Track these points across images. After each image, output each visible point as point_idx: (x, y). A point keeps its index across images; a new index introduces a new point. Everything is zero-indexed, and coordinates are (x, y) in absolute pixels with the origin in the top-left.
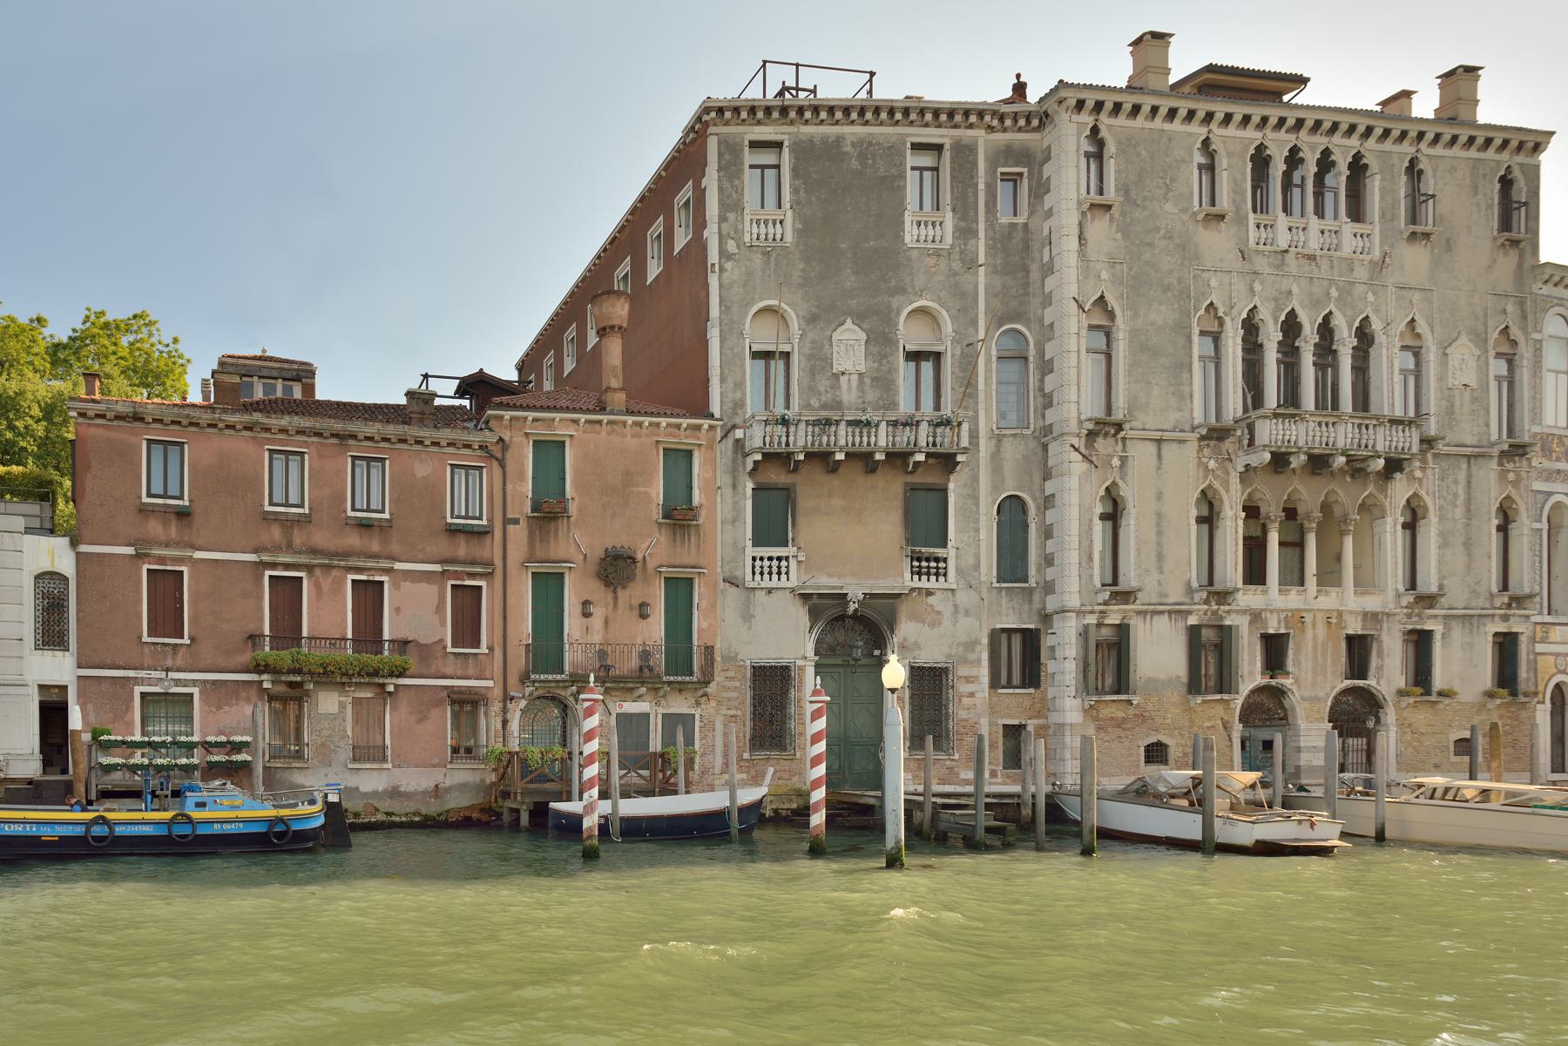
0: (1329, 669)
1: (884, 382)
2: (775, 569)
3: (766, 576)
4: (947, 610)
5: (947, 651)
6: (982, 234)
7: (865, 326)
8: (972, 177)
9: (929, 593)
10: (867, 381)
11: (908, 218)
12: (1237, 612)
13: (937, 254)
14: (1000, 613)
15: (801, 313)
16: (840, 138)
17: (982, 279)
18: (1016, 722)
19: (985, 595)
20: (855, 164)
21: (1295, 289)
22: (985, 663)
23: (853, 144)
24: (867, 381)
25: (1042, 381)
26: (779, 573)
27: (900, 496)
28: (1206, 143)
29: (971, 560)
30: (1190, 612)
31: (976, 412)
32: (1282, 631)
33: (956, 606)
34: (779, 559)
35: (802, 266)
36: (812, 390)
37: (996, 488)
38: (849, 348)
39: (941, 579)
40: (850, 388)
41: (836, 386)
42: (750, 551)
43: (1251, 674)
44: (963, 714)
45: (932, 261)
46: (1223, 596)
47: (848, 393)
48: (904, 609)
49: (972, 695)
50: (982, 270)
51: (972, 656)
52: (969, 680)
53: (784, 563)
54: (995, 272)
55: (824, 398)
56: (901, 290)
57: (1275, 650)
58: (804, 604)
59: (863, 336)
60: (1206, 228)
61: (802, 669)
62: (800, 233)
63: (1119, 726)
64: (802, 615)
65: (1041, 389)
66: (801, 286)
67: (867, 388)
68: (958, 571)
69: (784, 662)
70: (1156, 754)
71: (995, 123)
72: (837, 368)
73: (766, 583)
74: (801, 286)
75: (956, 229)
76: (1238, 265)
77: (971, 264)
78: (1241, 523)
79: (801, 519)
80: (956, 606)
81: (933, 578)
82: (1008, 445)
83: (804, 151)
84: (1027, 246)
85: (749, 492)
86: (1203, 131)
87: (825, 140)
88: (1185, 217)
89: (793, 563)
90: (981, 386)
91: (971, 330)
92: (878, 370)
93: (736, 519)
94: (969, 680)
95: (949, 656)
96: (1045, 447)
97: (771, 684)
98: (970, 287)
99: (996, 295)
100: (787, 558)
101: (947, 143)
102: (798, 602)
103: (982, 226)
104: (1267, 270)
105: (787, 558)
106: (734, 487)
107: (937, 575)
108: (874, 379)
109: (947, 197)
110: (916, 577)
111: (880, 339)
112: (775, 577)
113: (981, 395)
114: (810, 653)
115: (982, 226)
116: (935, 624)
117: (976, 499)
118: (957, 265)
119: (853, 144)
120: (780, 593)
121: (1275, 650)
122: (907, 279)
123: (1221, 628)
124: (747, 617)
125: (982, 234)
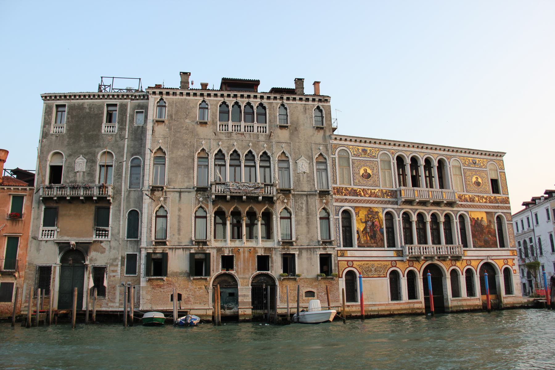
0: (250, 268)
1: (90, 173)
2: (50, 234)
4: (107, 248)
5: (106, 262)
6: (127, 129)
7: (87, 157)
9: (101, 242)
10: (86, 174)
11: (103, 126)
12: (212, 248)
13: (112, 135)
16: (83, 104)
19: (121, 242)
20: (87, 110)
21: (235, 144)
22: (120, 266)
27: (94, 210)
29: (116, 231)
30: (192, 248)
31: (121, 183)
32: (231, 254)
33: (110, 247)
34: (52, 231)
35: (68, 140)
37: (127, 208)
38: (81, 164)
39: (106, 237)
41: (75, 176)
42: (42, 228)
43: (217, 268)
45: (110, 137)
48: (93, 247)
49: (114, 276)
51: (115, 263)
52: (113, 271)
53: (53, 232)
55: (71, 180)
56: (99, 146)
57: (228, 262)
59: (85, 160)
60: (201, 126)
61: (55, 267)
63: (160, 287)
64: (56, 249)
66: (67, 146)
68: (112, 235)
69: (48, 265)
71: (133, 98)
72: (76, 170)
73: (46, 239)
74: (67, 146)
76: (213, 136)
77: (122, 138)
79: (60, 219)
81: (104, 237)
82: (132, 194)
83: (72, 108)
85: (43, 209)
89: (56, 233)
90: (124, 175)
91: (121, 158)
93: (38, 218)
94: (113, 271)
95: (107, 263)
97: (44, 273)
98: (122, 145)
99: (132, 147)
101: (118, 104)
103: (127, 127)
104: (225, 138)
106: (38, 208)
107: (105, 236)
110: (98, 237)
111: (91, 161)
112: (49, 236)
115: (127, 127)
116: (103, 252)
117: (120, 211)
118: (118, 139)
121: (228, 262)
122: (101, 143)
124: (38, 250)
125: (127, 129)
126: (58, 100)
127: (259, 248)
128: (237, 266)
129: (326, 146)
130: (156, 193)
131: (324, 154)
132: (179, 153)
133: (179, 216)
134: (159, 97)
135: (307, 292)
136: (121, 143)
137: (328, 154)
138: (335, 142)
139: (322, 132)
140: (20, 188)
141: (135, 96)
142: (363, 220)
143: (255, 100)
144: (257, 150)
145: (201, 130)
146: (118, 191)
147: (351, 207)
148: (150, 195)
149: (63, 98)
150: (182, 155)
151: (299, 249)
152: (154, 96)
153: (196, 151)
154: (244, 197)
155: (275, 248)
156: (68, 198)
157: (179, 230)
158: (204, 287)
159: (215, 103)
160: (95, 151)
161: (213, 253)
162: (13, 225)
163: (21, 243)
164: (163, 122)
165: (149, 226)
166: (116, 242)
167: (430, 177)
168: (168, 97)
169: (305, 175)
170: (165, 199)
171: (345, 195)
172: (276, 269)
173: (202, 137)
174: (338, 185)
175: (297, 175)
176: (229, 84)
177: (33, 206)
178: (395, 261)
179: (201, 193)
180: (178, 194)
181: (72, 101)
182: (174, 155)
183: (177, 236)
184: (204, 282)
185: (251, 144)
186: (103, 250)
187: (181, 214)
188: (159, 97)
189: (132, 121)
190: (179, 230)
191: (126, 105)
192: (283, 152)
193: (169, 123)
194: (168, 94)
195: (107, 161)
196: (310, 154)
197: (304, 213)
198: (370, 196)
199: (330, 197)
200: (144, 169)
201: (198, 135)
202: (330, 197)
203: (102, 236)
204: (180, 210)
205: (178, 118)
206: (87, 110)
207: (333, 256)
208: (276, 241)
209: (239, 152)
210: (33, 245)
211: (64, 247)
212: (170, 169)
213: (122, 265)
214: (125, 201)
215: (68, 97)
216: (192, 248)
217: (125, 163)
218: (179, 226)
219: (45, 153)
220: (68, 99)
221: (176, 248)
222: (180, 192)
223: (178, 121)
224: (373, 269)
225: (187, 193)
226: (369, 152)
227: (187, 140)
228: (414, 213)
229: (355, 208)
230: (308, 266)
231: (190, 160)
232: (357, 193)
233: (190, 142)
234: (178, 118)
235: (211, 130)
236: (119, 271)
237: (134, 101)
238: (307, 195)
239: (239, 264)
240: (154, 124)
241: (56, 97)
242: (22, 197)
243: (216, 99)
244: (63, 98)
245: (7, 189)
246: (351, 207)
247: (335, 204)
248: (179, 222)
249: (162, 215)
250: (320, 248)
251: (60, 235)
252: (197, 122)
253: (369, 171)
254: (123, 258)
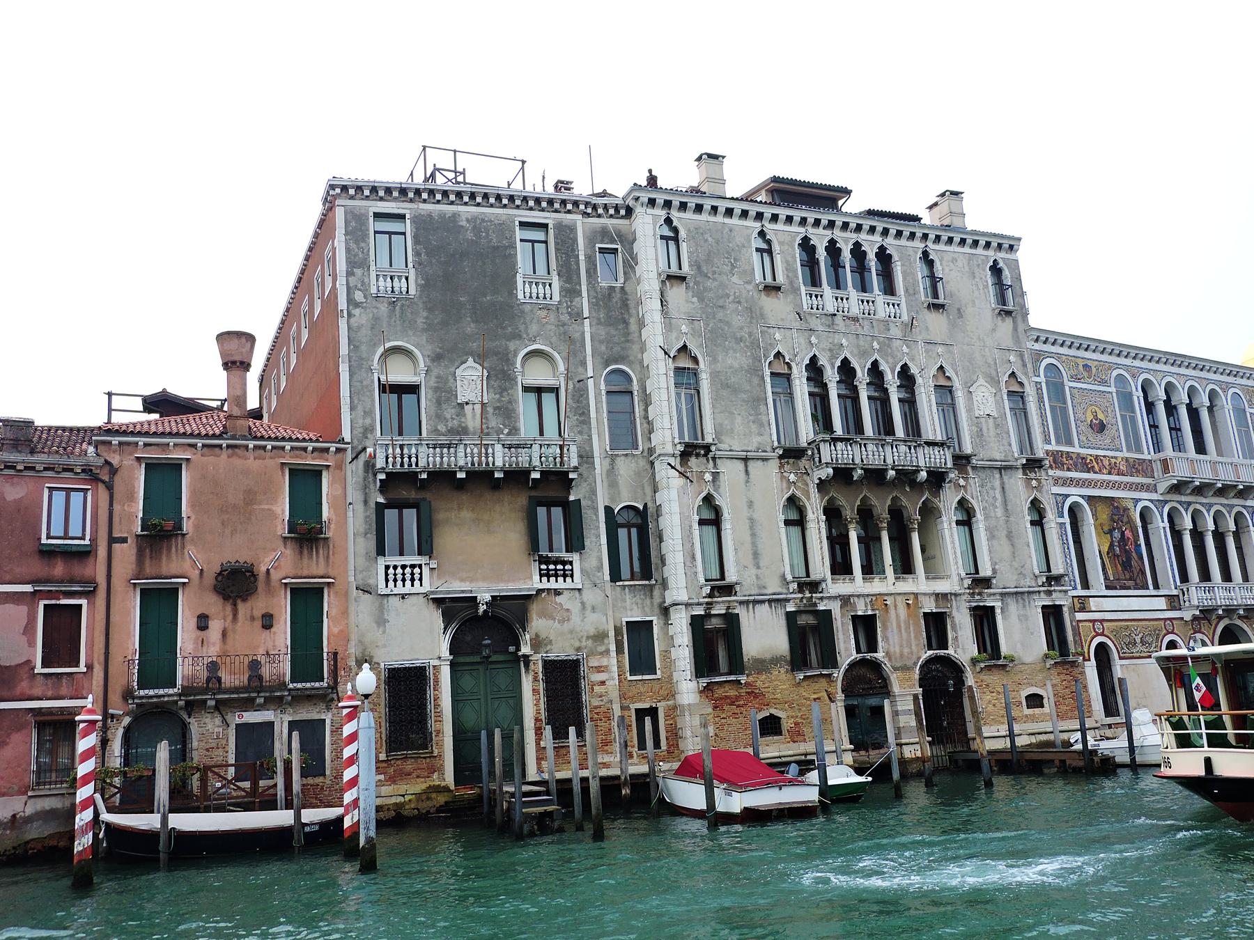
3: (400, 583)
6: (585, 294)
8: (573, 250)
9: (557, 592)
10: (490, 410)
12: (829, 598)
13: (547, 308)
14: (625, 608)
15: (427, 353)
16: (455, 215)
17: (587, 329)
18: (646, 706)
20: (470, 235)
21: (844, 342)
22: (614, 654)
23: (468, 220)
24: (490, 410)
25: (646, 410)
26: (413, 580)
28: (762, 234)
30: (788, 600)
31: (590, 436)
32: (870, 612)
33: (583, 603)
34: (413, 566)
35: (425, 314)
36: (439, 417)
38: (470, 381)
40: (474, 416)
43: (847, 649)
44: (596, 702)
45: (543, 313)
46: (814, 586)
47: (472, 419)
48: (534, 608)
49: (603, 683)
50: (587, 322)
52: (599, 669)
53: (417, 570)
54: (599, 323)
56: (517, 336)
58: (438, 607)
60: (768, 295)
62: (425, 287)
64: (436, 618)
65: (646, 417)
67: (490, 416)
69: (418, 663)
70: (771, 726)
71: (589, 210)
73: (400, 589)
74: (424, 330)
75: (562, 289)
76: (797, 324)
77: (577, 316)
78: (823, 525)
80: (583, 603)
81: (561, 579)
82: (620, 462)
83: (423, 224)
84: (625, 304)
86: (758, 225)
87: (442, 215)
88: (750, 287)
89: (426, 570)
90: (593, 414)
91: (580, 369)
92: (499, 401)
94: (599, 669)
95: (578, 649)
96: (652, 463)
97: (406, 687)
99: (601, 342)
100: (420, 566)
102: (432, 606)
103: (584, 288)
105: (420, 566)
107: (565, 576)
108: (495, 408)
109: (553, 265)
110: (545, 579)
111: (500, 376)
112: (408, 583)
113: (594, 422)
114: (445, 651)
115: (584, 288)
118: (565, 318)
119: (468, 220)
120: (414, 598)
122: (522, 328)
123: (816, 613)
124: (381, 621)
125: (585, 294)
126: (381, 199)
127: (925, 594)
128: (886, 638)
129: (1021, 356)
130: (693, 461)
131: (1018, 374)
132: (729, 361)
133: (752, 520)
134: (662, 213)
135: (1028, 698)
136: (573, 329)
137: (1026, 374)
138: (1037, 346)
139: (1009, 321)
140: (310, 446)
141: (595, 207)
142: (1106, 528)
143: (870, 237)
144: (891, 360)
145: (777, 308)
146: (586, 457)
147: (1082, 497)
148: (678, 467)
149: (395, 194)
150: (736, 365)
151: (1002, 594)
152: (650, 211)
153: (766, 357)
154: (892, 473)
155: (956, 595)
156: (461, 475)
157: (756, 555)
158: (825, 694)
159: (788, 238)
160: (507, 348)
161: (835, 607)
162: (301, 553)
163: (329, 603)
164: (683, 279)
165: (688, 546)
166: (597, 590)
167: (1175, 429)
168: (682, 215)
169: (991, 421)
170: (716, 475)
171: (1069, 470)
172: (963, 646)
173: (773, 323)
174: (1053, 447)
175: (976, 421)
176: (787, 192)
177: (349, 500)
178: (1171, 619)
179: (791, 461)
180: (740, 465)
181: (422, 206)
182: (719, 367)
183: (753, 571)
184: (823, 683)
185: (876, 345)
186: (565, 614)
187: (755, 516)
188: (662, 213)
189: (592, 272)
190: (756, 555)
191: (572, 229)
192: (941, 367)
193: (697, 283)
194: (683, 206)
195: (538, 375)
196: (994, 374)
197: (1000, 512)
198: (1110, 473)
199: (1043, 473)
200: (647, 400)
201: (762, 316)
202: (1043, 473)
203: (556, 576)
204: (750, 504)
205: (714, 273)
206: (470, 235)
207: (1065, 609)
208: (955, 578)
209: (855, 364)
210: (363, 609)
211: (454, 609)
212: (715, 400)
213: (619, 650)
214: (605, 484)
215: (411, 195)
216: (788, 600)
217: (591, 382)
218: (754, 544)
219: (363, 348)
220: (411, 201)
221: (756, 602)
222: (746, 460)
223: (714, 279)
224: (1138, 640)
225: (760, 463)
226: (1094, 370)
227: (742, 328)
228: (1186, 510)
229: (1090, 499)
230: (1022, 634)
231: (756, 381)
232: (1086, 464)
233: (750, 334)
234: (714, 273)
235: (790, 308)
236: (615, 669)
237: (591, 220)
238: (1000, 469)
239: (889, 634)
240: (663, 282)
241: (374, 189)
242: (316, 474)
243: (788, 228)
244: (395, 194)
245: (274, 448)
246: (1082, 497)
247: (1056, 490)
248: (753, 535)
249: (712, 518)
250: (1039, 592)
251: (439, 577)
252: (758, 285)
253: (1101, 416)
254: (618, 631)
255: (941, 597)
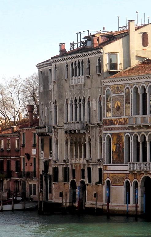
133: (61, 144)
142: (115, 143)
161: (70, 166)
171: (108, 125)
180: (60, 129)
198: (119, 125)
229: (112, 134)
253: (119, 105)
255: (84, 165)
